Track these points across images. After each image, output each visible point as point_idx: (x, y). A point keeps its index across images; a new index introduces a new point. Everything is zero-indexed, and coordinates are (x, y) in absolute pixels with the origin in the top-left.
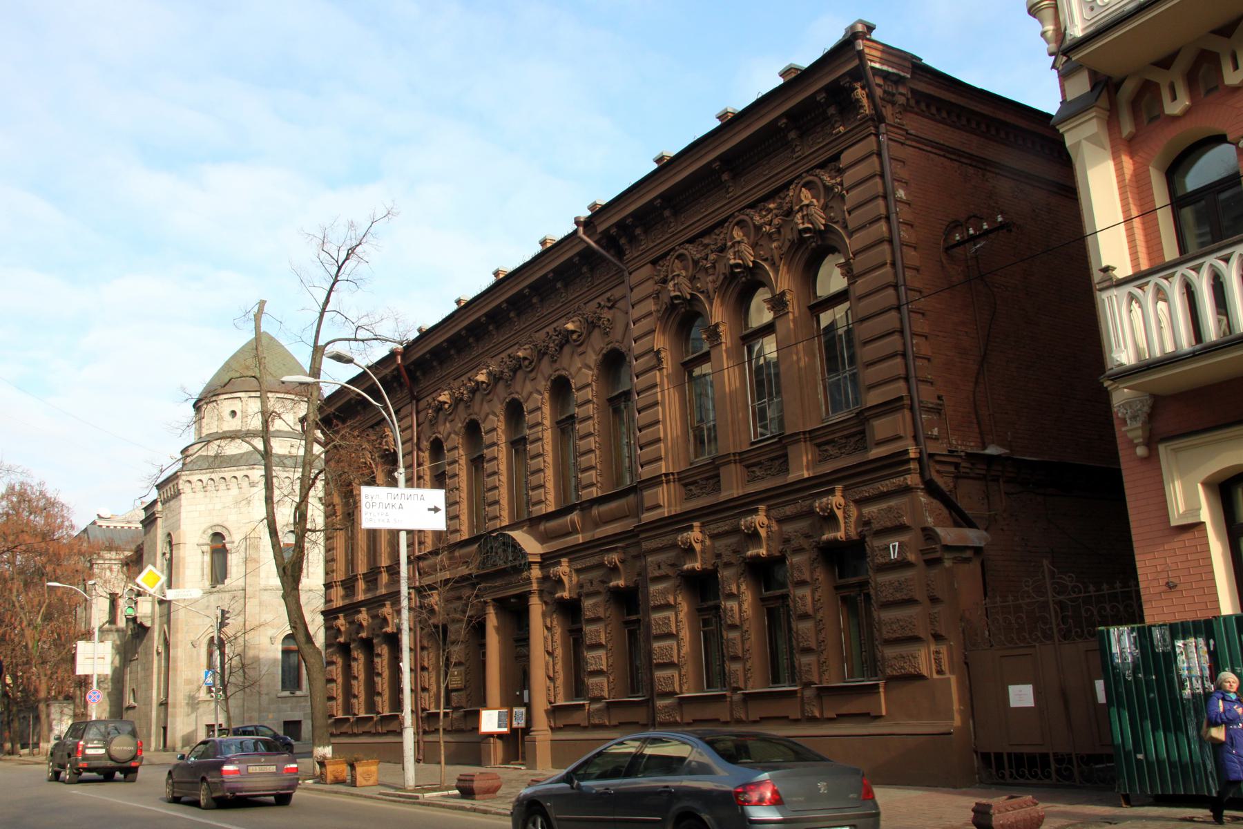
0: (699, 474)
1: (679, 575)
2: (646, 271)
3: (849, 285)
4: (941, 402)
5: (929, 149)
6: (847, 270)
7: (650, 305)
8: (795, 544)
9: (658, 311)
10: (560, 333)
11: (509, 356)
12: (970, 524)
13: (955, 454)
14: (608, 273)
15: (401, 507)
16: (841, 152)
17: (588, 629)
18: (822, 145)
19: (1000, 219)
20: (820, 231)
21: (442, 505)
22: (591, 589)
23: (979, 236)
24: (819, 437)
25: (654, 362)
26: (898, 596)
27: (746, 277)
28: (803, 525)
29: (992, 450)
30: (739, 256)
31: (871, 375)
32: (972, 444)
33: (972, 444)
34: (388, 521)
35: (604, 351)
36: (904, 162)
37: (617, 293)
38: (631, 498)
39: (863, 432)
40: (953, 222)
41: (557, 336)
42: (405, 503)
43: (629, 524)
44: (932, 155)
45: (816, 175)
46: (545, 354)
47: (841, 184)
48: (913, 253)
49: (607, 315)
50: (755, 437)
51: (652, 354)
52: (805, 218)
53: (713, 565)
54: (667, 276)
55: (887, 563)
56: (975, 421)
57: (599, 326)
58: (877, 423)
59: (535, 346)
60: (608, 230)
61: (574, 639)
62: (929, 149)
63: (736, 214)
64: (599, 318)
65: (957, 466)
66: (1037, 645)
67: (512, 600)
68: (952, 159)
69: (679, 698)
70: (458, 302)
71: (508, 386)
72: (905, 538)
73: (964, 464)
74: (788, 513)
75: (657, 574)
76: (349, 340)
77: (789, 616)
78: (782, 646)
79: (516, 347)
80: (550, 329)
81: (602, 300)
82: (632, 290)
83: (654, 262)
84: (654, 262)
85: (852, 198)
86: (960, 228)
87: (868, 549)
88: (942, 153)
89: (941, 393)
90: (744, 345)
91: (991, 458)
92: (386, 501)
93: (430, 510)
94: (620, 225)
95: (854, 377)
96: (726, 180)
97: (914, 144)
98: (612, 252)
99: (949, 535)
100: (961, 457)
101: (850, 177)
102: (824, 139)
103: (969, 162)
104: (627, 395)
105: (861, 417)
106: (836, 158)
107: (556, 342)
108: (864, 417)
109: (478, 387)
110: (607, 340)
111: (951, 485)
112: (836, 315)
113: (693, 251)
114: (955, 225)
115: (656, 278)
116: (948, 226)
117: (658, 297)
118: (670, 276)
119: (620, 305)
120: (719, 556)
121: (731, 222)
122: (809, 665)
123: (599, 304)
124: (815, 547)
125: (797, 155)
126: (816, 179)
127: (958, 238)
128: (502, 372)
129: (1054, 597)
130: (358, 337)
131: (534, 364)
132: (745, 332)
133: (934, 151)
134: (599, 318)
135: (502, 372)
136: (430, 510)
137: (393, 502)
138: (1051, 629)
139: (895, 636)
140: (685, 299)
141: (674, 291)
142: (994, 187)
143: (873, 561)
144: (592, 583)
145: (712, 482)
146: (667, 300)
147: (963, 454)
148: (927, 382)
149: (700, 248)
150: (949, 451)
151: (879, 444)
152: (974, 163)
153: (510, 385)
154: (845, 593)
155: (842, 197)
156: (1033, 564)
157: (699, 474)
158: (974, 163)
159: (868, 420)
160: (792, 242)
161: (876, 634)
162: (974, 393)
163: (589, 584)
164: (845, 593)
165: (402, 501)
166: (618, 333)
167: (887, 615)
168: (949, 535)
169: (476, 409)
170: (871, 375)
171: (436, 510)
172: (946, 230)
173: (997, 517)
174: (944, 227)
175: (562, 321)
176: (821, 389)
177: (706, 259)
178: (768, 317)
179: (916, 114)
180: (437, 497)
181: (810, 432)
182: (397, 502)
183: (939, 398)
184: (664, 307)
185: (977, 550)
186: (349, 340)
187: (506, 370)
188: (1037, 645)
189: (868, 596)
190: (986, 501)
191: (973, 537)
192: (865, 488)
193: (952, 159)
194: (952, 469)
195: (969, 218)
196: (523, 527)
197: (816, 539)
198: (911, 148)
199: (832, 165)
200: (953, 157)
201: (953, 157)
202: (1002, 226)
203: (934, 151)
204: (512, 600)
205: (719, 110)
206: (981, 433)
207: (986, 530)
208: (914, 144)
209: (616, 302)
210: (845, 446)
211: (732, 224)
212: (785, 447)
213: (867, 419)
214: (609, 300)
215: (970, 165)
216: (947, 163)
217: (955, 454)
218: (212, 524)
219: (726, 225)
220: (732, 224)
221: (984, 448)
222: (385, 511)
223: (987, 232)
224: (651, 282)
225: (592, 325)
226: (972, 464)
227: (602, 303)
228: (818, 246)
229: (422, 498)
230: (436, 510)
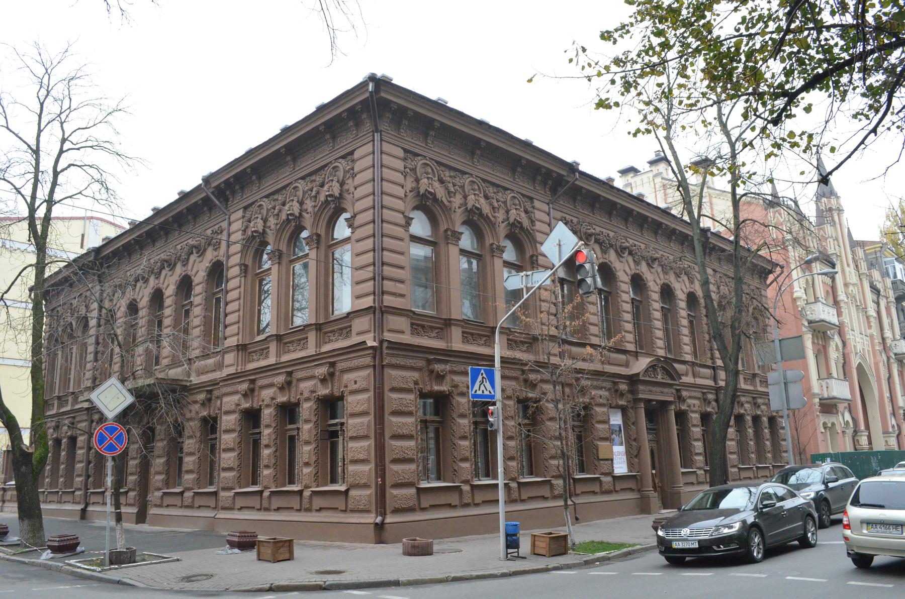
3: (352, 233)
6: (350, 223)
16: (355, 150)
47: (353, 169)
60: (219, 185)
83: (246, 208)
85: (359, 179)
94: (227, 182)
98: (222, 199)
101: (358, 166)
106: (352, 153)
146: (250, 233)
151: (359, 334)
199: (349, 157)
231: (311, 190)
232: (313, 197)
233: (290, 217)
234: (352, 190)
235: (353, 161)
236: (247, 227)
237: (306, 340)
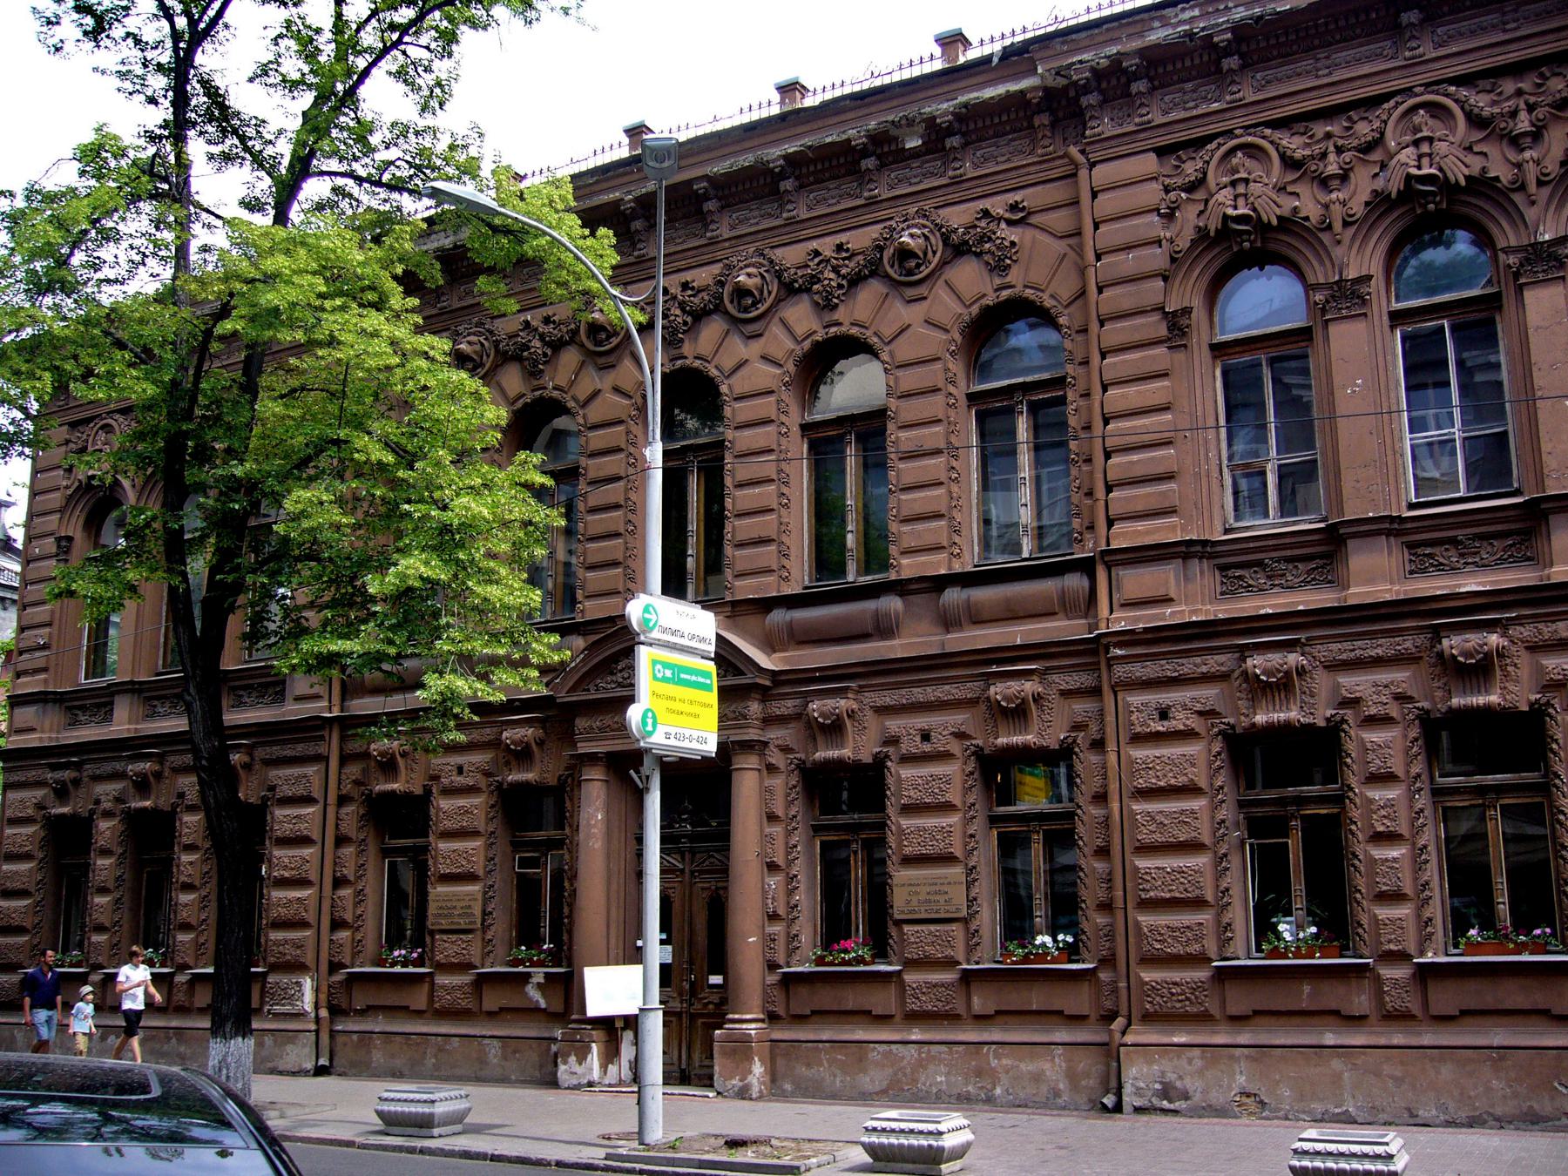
0: (1276, 548)
1: (1220, 733)
14: (1009, 160)
22: (927, 747)
25: (1163, 331)
27: (1436, 204)
38: (1075, 582)
53: (1328, 720)
57: (978, 255)
61: (822, 843)
64: (985, 238)
75: (1160, 727)
80: (826, 246)
81: (997, 206)
107: (844, 271)
110: (998, 281)
113: (1294, 144)
119: (1034, 220)
121: (1398, 104)
157: (1276, 548)
163: (918, 739)
214: (1014, 207)
224: (1156, 186)
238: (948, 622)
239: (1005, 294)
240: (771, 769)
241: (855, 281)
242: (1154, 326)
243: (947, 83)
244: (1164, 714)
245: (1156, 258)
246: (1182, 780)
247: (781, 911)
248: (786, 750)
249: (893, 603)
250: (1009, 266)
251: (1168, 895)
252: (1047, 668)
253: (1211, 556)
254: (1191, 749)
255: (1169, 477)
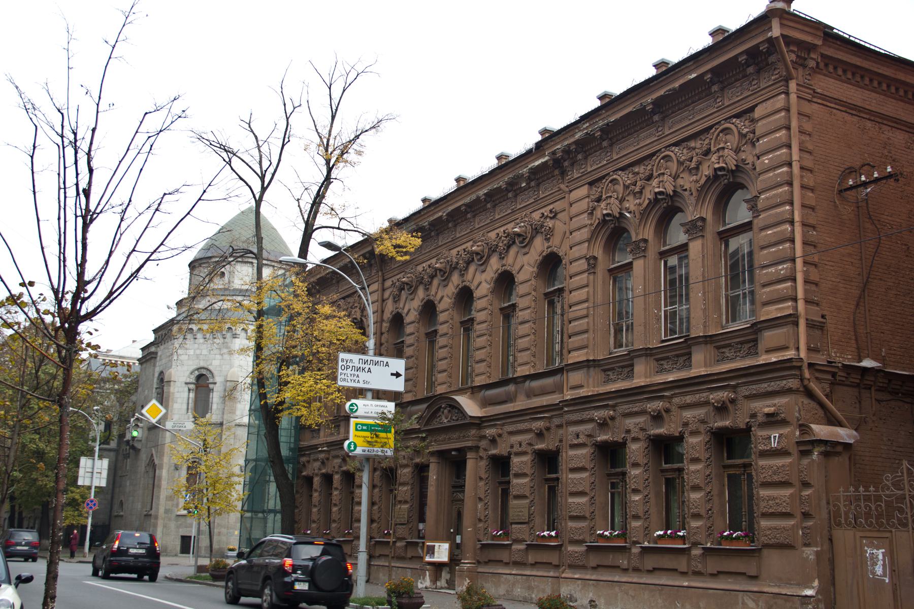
1: (593, 444)
2: (584, 191)
3: (754, 217)
4: (824, 321)
5: (832, 105)
6: (753, 204)
7: (584, 219)
8: (692, 427)
9: (591, 225)
10: (508, 235)
11: (464, 250)
12: (840, 425)
13: (833, 364)
14: (552, 189)
15: (369, 370)
16: (756, 106)
17: (515, 481)
18: (739, 98)
19: (889, 169)
20: (732, 171)
21: (402, 372)
22: (520, 449)
23: (871, 182)
24: (719, 341)
25: (586, 267)
26: (776, 478)
28: (701, 412)
29: (867, 363)
30: (663, 185)
31: (764, 293)
32: (850, 357)
33: (850, 357)
34: (358, 381)
35: (544, 254)
36: (809, 117)
37: (558, 206)
39: (755, 341)
40: (848, 169)
41: (506, 237)
42: (373, 367)
43: (555, 398)
44: (835, 111)
45: (733, 124)
46: (494, 251)
48: (811, 194)
49: (550, 223)
50: (666, 336)
51: (584, 261)
52: (721, 159)
54: (601, 196)
55: (767, 451)
56: (853, 338)
58: (767, 334)
59: (487, 244)
62: (832, 105)
63: (663, 150)
65: (834, 375)
66: (893, 530)
67: (453, 453)
68: (852, 114)
69: (587, 546)
70: (424, 200)
71: (462, 275)
72: (785, 431)
73: (840, 373)
74: (688, 401)
76: (333, 228)
77: (683, 486)
78: (675, 511)
79: (471, 243)
81: (546, 211)
82: (571, 205)
84: (591, 184)
86: (854, 173)
87: (753, 439)
88: (844, 109)
89: (825, 313)
90: (661, 259)
91: (865, 370)
92: (357, 365)
93: (392, 374)
95: (752, 293)
96: (656, 121)
97: (819, 101)
99: (821, 431)
100: (838, 367)
101: (760, 128)
102: (742, 94)
103: (868, 117)
104: (561, 291)
105: (755, 328)
106: (752, 109)
107: (505, 242)
108: (757, 328)
109: (436, 274)
111: (828, 390)
112: (739, 243)
114: (851, 171)
115: (592, 197)
116: (844, 172)
117: (592, 214)
118: (604, 197)
119: (559, 216)
120: (628, 431)
122: (697, 528)
123: (543, 214)
124: (709, 431)
125: (718, 105)
126: (732, 127)
127: (851, 183)
128: (457, 263)
129: (910, 492)
130: (341, 227)
131: (484, 259)
132: (663, 249)
133: (837, 107)
134: (542, 226)
135: (457, 263)
136: (392, 374)
137: (364, 366)
138: (906, 518)
139: (771, 511)
140: (614, 217)
141: (606, 209)
142: (889, 139)
143: (755, 447)
144: (520, 445)
145: (626, 370)
147: (840, 365)
148: (814, 303)
149: (630, 176)
150: (829, 362)
151: (768, 351)
152: (872, 118)
153: (463, 274)
154: (732, 471)
155: (753, 145)
156: (897, 461)
158: (872, 118)
159: (761, 331)
160: (708, 178)
161: (755, 508)
162: (855, 313)
164: (732, 471)
165: (371, 366)
166: (556, 240)
167: (764, 493)
168: (821, 431)
169: (433, 292)
170: (764, 293)
171: (397, 375)
172: (841, 175)
173: (867, 419)
174: (840, 173)
175: (512, 224)
176: (723, 301)
177: (635, 185)
178: (682, 238)
179: (825, 75)
180: (399, 365)
181: (711, 336)
182: (367, 366)
183: (823, 317)
184: (597, 221)
185: (847, 446)
186: (333, 228)
187: (461, 262)
188: (893, 530)
189: (750, 477)
190: (858, 406)
191: (845, 434)
192: (754, 387)
193: (852, 114)
194: (829, 377)
195: (863, 166)
196: (466, 393)
197: (711, 425)
198: (816, 105)
200: (854, 112)
201: (854, 112)
202: (890, 176)
203: (837, 107)
204: (453, 453)
205: (657, 59)
206: (858, 348)
207: (856, 430)
208: (819, 101)
209: (556, 214)
210: (740, 351)
211: (659, 158)
212: (689, 347)
213: (760, 330)
214: (551, 211)
215: (869, 120)
216: (848, 117)
217: (833, 364)
218: (198, 366)
219: (654, 158)
220: (659, 158)
221: (860, 361)
222: (356, 373)
223: (877, 180)
224: (587, 200)
225: (537, 230)
226: (849, 374)
227: (546, 214)
228: (729, 182)
229: (387, 364)
230: (397, 375)
231: (691, 160)
232: (693, 168)
233: (659, 197)
234: (750, 159)
235: (753, 121)
236: (594, 209)
237: (687, 357)
238: (530, 394)
239: (549, 250)
240: (481, 458)
241: (509, 247)
242: (582, 265)
243: (524, 160)
244: (578, 436)
245: (584, 234)
246: (581, 465)
247: (482, 518)
248: (485, 450)
249: (511, 388)
250: (549, 238)
251: (575, 514)
252: (552, 416)
253: (599, 366)
254: (584, 451)
255: (586, 331)
